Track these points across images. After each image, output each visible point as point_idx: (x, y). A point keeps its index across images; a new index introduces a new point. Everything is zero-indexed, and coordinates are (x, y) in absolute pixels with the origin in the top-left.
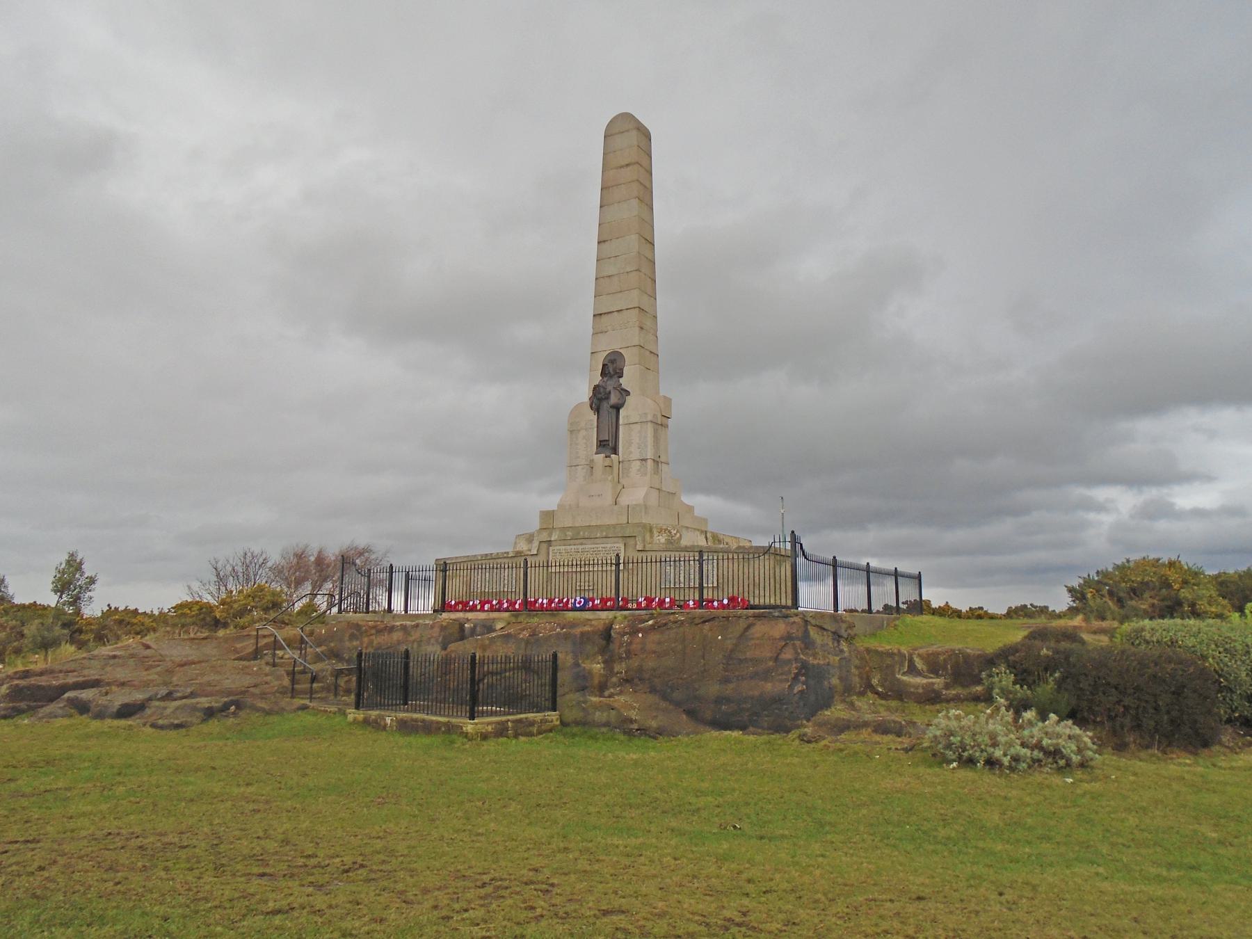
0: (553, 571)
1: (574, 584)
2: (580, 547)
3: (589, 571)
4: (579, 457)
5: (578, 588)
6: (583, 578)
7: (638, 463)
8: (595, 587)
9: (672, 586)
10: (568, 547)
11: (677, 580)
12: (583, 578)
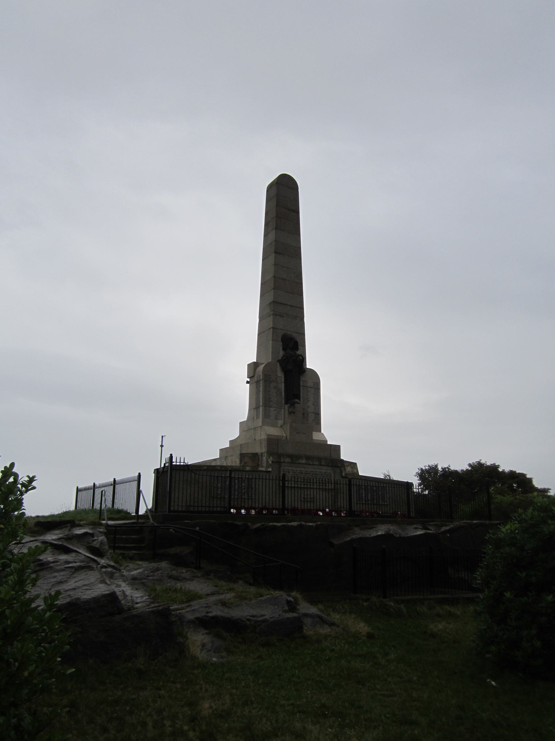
0: (330, 488)
1: (299, 496)
2: (302, 469)
3: (310, 488)
4: (271, 401)
5: (303, 500)
6: (306, 493)
7: (313, 414)
8: (315, 500)
9: (364, 502)
10: (294, 469)
12: (306, 493)
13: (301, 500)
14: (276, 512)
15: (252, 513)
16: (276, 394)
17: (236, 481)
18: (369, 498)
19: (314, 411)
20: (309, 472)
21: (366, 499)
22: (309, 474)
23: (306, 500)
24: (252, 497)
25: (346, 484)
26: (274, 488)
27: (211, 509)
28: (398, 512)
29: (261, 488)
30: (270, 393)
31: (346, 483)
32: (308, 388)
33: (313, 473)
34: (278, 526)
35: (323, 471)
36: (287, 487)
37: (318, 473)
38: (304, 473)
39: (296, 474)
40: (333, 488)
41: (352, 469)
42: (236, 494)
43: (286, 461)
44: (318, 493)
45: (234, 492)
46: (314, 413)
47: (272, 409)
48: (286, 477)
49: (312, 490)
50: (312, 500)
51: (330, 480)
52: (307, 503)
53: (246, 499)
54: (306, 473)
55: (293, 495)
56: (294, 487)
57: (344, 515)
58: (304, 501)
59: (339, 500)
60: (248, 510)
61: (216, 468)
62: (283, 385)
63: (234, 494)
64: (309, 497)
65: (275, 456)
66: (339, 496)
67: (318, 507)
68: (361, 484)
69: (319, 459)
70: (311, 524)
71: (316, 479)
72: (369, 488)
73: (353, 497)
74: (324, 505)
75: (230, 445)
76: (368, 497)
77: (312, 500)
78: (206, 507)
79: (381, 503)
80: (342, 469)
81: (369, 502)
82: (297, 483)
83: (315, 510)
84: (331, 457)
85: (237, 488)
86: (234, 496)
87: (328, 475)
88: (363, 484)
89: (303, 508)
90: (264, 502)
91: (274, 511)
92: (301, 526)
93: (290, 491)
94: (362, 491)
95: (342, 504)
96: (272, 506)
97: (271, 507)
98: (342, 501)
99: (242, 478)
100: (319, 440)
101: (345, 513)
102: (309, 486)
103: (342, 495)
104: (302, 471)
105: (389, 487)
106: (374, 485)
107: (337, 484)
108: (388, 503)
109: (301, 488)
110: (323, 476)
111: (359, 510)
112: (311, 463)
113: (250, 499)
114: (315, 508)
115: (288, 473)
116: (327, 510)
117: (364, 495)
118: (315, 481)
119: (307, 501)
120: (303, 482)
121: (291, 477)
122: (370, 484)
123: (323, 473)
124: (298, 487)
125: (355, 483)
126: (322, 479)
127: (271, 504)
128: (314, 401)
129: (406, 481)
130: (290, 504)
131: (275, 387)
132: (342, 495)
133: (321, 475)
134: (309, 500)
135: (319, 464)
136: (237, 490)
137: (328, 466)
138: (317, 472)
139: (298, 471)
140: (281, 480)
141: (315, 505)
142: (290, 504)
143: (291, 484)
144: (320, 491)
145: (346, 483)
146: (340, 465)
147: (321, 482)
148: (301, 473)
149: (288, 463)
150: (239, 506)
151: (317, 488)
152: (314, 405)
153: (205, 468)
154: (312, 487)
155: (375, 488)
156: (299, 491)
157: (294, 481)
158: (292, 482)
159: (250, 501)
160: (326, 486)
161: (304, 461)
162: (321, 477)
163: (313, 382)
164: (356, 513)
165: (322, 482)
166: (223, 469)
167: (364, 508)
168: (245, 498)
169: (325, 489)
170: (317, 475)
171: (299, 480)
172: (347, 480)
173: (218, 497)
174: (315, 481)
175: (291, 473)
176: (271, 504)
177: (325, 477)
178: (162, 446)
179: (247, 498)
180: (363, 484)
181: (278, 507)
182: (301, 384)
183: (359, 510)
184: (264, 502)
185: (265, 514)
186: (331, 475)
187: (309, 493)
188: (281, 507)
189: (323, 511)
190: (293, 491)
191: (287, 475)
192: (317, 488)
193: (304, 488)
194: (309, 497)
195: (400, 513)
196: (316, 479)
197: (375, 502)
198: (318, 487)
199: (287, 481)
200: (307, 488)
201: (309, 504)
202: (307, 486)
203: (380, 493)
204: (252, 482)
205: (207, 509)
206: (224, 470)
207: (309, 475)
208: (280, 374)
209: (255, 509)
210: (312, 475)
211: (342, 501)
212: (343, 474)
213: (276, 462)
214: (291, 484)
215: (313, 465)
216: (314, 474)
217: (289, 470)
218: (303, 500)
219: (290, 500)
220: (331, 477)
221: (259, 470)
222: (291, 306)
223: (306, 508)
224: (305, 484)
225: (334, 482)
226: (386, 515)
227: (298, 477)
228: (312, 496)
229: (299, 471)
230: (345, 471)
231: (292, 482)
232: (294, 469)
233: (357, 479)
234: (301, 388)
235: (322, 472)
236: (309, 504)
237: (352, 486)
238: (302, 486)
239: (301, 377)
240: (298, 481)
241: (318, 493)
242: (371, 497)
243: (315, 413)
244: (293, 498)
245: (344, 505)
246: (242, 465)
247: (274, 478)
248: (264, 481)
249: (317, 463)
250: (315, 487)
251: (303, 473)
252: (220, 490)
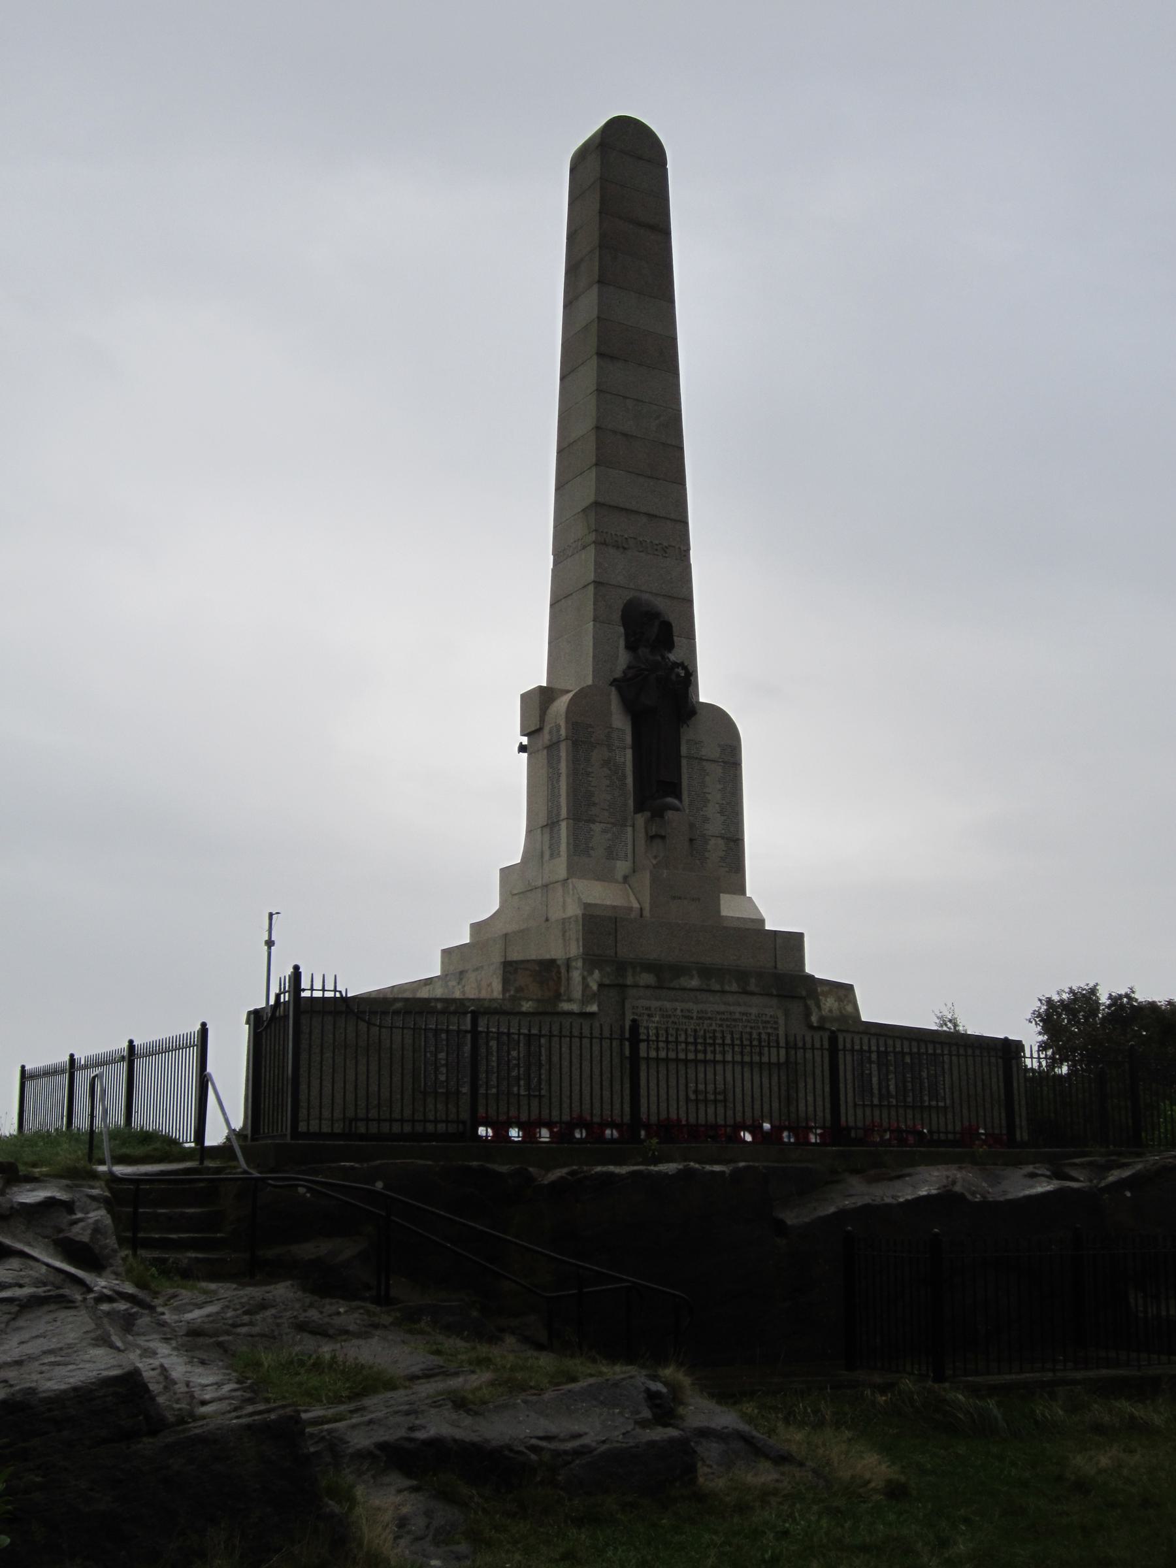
1: (682, 1087)
2: (690, 1006)
3: (715, 1062)
4: (595, 804)
5: (692, 1096)
6: (701, 1076)
7: (720, 841)
8: (730, 1096)
9: (876, 1101)
10: (668, 1005)
11: (884, 1091)
12: (701, 1076)
13: (687, 1099)
14: (612, 1134)
15: (540, 1137)
16: (608, 782)
17: (493, 1044)
18: (892, 1088)
19: (723, 831)
20: (709, 1015)
21: (884, 1091)
22: (710, 1018)
23: (701, 1097)
24: (540, 1090)
25: (822, 1049)
26: (606, 1063)
27: (419, 1128)
28: (978, 1128)
29: (566, 1063)
30: (591, 779)
31: (822, 1045)
32: (704, 763)
33: (723, 1017)
34: (619, 1175)
35: (754, 1011)
36: (644, 1058)
37: (737, 1016)
38: (697, 1017)
39: (671, 1020)
40: (782, 1060)
41: (839, 1004)
42: (494, 1082)
43: (642, 983)
44: (738, 1076)
45: (487, 1077)
46: (723, 838)
47: (597, 828)
48: (642, 1030)
49: (719, 1068)
50: (720, 1097)
51: (775, 1038)
52: (706, 1106)
53: (524, 1095)
54: (700, 1018)
55: (663, 1084)
56: (667, 1060)
57: (816, 1138)
58: (697, 1101)
59: (801, 1094)
60: (528, 1128)
61: (433, 1004)
62: (629, 753)
63: (487, 1083)
64: (710, 1088)
65: (608, 969)
66: (801, 1085)
67: (739, 1119)
68: (865, 1048)
69: (742, 976)
70: (717, 1168)
71: (732, 1033)
72: (891, 1057)
73: (842, 1086)
74: (757, 1113)
75: (472, 935)
76: (888, 1086)
77: (720, 1097)
78: (402, 1121)
79: (927, 1104)
80: (811, 1003)
81: (891, 1100)
82: (675, 1047)
83: (730, 1126)
84: (776, 968)
85: (495, 1064)
86: (487, 1090)
87: (768, 1022)
88: (874, 1048)
89: (692, 1120)
90: (576, 1105)
91: (608, 1132)
92: (687, 1174)
93: (653, 1072)
94: (870, 1070)
95: (811, 1109)
96: (601, 1115)
97: (597, 1119)
98: (810, 1099)
99: (509, 1034)
100: (738, 918)
101: (821, 1135)
102: (710, 1056)
103: (810, 1081)
104: (689, 1011)
105: (950, 1055)
106: (906, 1050)
107: (796, 1047)
108: (948, 1102)
109: (686, 1061)
110: (753, 1025)
111: (860, 1124)
112: (717, 987)
113: (535, 1096)
114: (730, 1122)
115: (646, 1017)
116: (767, 1126)
117: (875, 1080)
118: (728, 1041)
119: (706, 1101)
120: (692, 1043)
121: (657, 1031)
122: (894, 1047)
123: (753, 1018)
124: (677, 1060)
125: (848, 1046)
126: (751, 1034)
127: (597, 1111)
128: (724, 802)
129: (1002, 1037)
130: (654, 1108)
131: (606, 763)
132: (810, 1081)
133: (746, 1024)
134: (712, 1097)
135: (740, 990)
136: (495, 1070)
137: (770, 995)
138: (735, 1013)
139: (678, 1012)
140: (627, 1039)
141: (730, 1113)
142: (654, 1108)
143: (657, 1049)
144: (745, 1069)
145: (822, 1045)
146: (804, 993)
147: (745, 1043)
148: (686, 1017)
149: (647, 987)
150: (503, 1118)
151: (734, 1062)
152: (722, 812)
153: (399, 1005)
154: (719, 1057)
155: (908, 1060)
156: (682, 1072)
157: (667, 1042)
158: (661, 1045)
159: (535, 1103)
160: (761, 1054)
161: (695, 983)
162: (748, 1030)
163: (719, 745)
164: (853, 1134)
165: (751, 1042)
166: (452, 1008)
167: (877, 1119)
168: (519, 1095)
169: (761, 1064)
170: (733, 1023)
171: (682, 1038)
172: (826, 1035)
173: (440, 1091)
174: (728, 1041)
175: (657, 1019)
176: (597, 1111)
177: (759, 1028)
178: (270, 943)
179: (527, 1093)
180: (874, 1048)
181: (618, 1119)
182: (684, 750)
183: (860, 1124)
184: (576, 1105)
185: (581, 1141)
186: (776, 1023)
187: (710, 1076)
188: (627, 1119)
189: (755, 1129)
190: (663, 1070)
191: (645, 1024)
192: (734, 1062)
193: (696, 1061)
194: (710, 1088)
195: (985, 1129)
196: (732, 1033)
197: (910, 1099)
198: (738, 1058)
199: (643, 1041)
200: (705, 1062)
201: (711, 1110)
202: (705, 1057)
203: (924, 1074)
204: (540, 1046)
205: (407, 1128)
206: (455, 1013)
207: (708, 1021)
208: (620, 722)
209: (549, 1125)
210: (719, 1022)
211: (810, 1099)
212: (814, 1019)
213: (608, 986)
214: (657, 1049)
215: (723, 992)
216: (727, 1020)
217: (649, 1008)
218: (692, 1096)
219: (653, 1099)
220: (776, 1029)
221: (559, 1010)
222: (651, 516)
223: (702, 1121)
224: (700, 1051)
225: (787, 1043)
226: (943, 1137)
227: (677, 1030)
228: (720, 1087)
229: (682, 1011)
230: (819, 1007)
231: (661, 1045)
232: (668, 1005)
233: (854, 1032)
234: (684, 762)
235: (750, 1014)
236: (711, 1110)
237: (841, 1054)
238: (691, 1056)
239: (682, 730)
240: (677, 1042)
241: (738, 1076)
242: (896, 1086)
243: (727, 839)
244: (663, 1092)
245: (815, 1110)
246: (510, 996)
247: (606, 1033)
248: (576, 1041)
249: (734, 987)
250: (729, 1058)
251: (692, 1018)
252: (444, 1070)
